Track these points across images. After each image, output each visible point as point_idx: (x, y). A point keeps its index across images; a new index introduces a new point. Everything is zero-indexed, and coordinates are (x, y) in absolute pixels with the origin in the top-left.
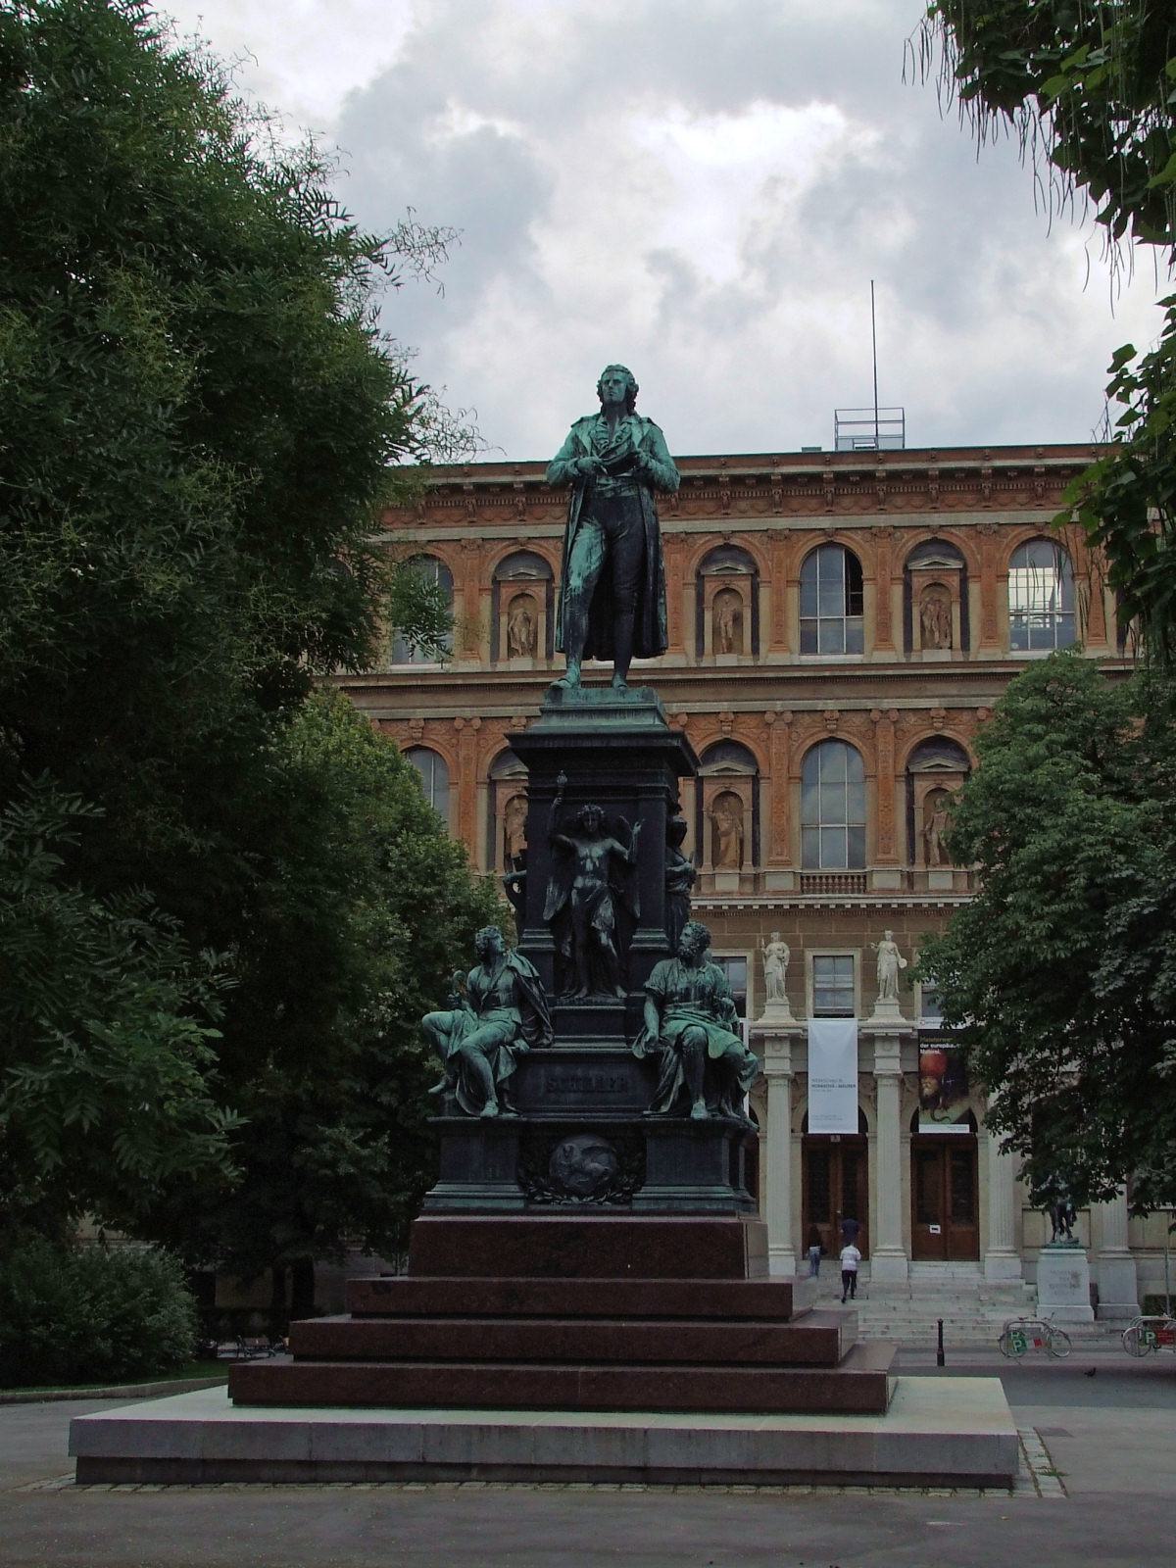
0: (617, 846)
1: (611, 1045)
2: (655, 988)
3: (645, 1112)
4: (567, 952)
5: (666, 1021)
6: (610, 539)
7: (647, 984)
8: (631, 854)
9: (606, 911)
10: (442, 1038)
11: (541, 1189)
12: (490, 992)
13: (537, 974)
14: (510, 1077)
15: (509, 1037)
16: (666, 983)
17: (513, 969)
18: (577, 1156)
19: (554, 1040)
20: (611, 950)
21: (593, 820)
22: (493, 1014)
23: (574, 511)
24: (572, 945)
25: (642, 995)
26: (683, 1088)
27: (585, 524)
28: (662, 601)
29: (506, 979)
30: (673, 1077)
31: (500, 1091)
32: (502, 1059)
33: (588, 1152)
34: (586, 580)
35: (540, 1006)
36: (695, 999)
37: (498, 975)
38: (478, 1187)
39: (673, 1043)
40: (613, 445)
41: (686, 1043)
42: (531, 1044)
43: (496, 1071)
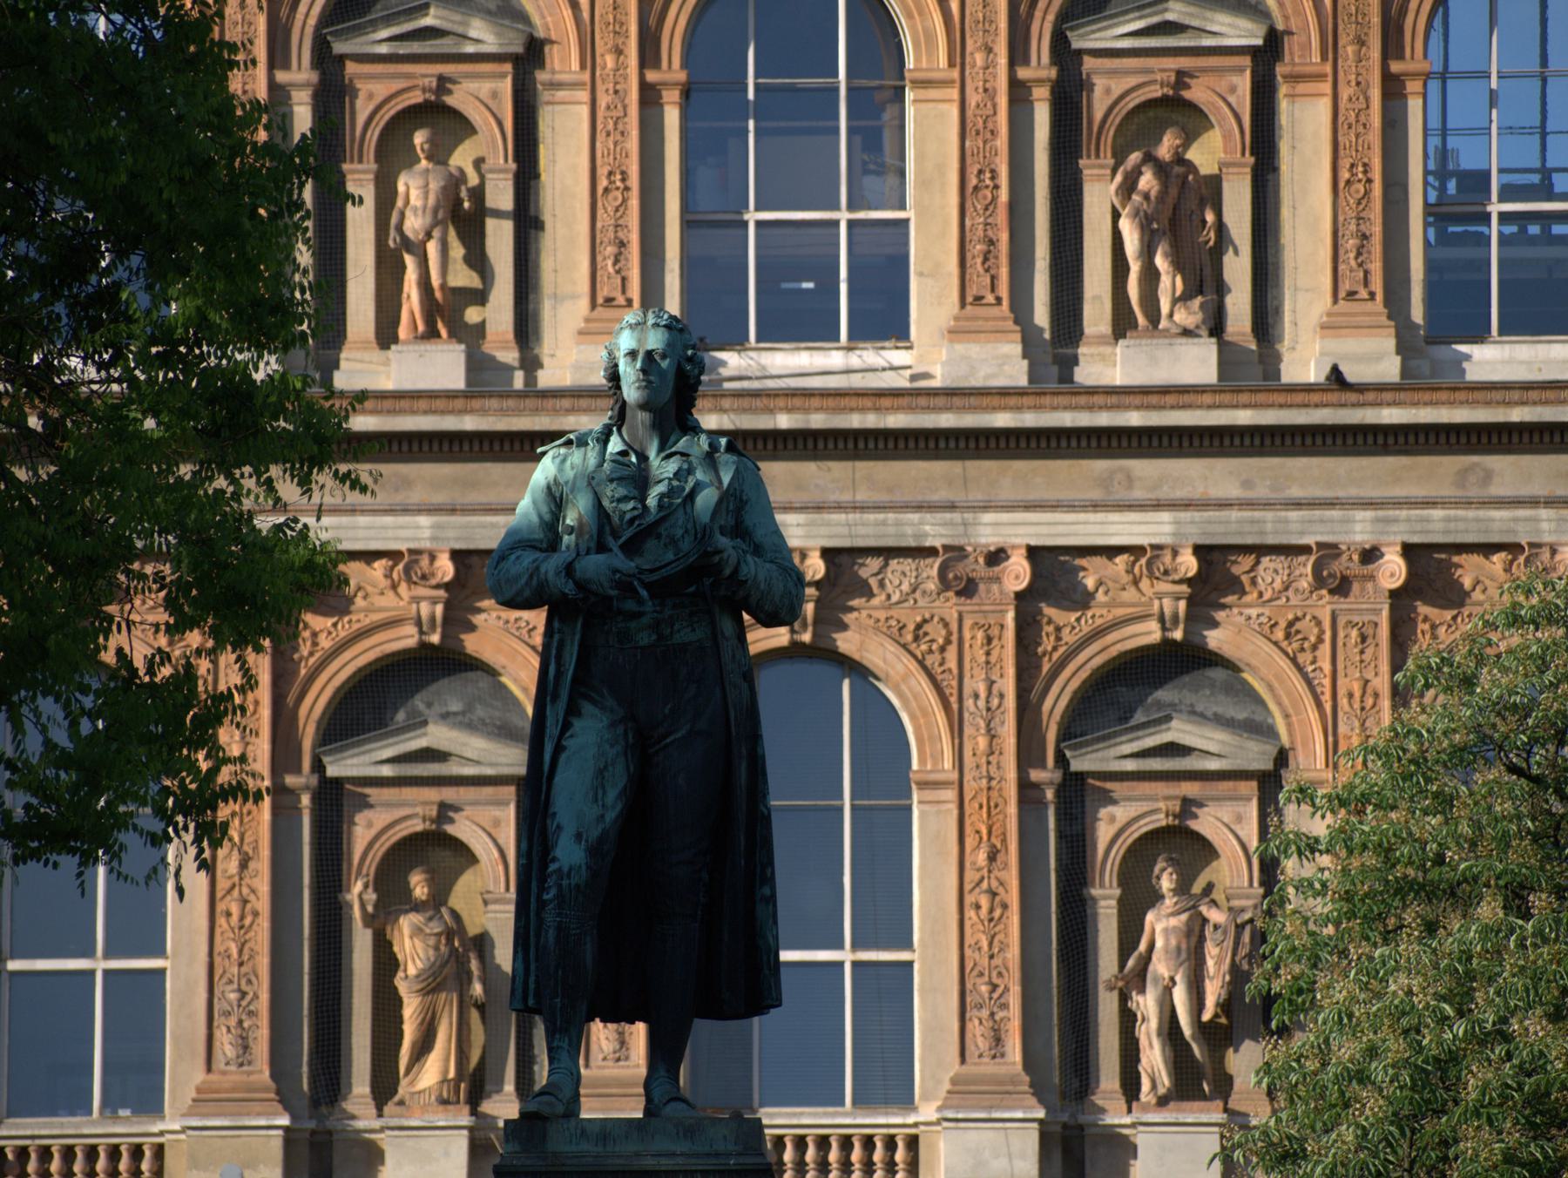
23: (559, 674)
27: (587, 708)
28: (767, 891)
34: (594, 851)
40: (650, 519)
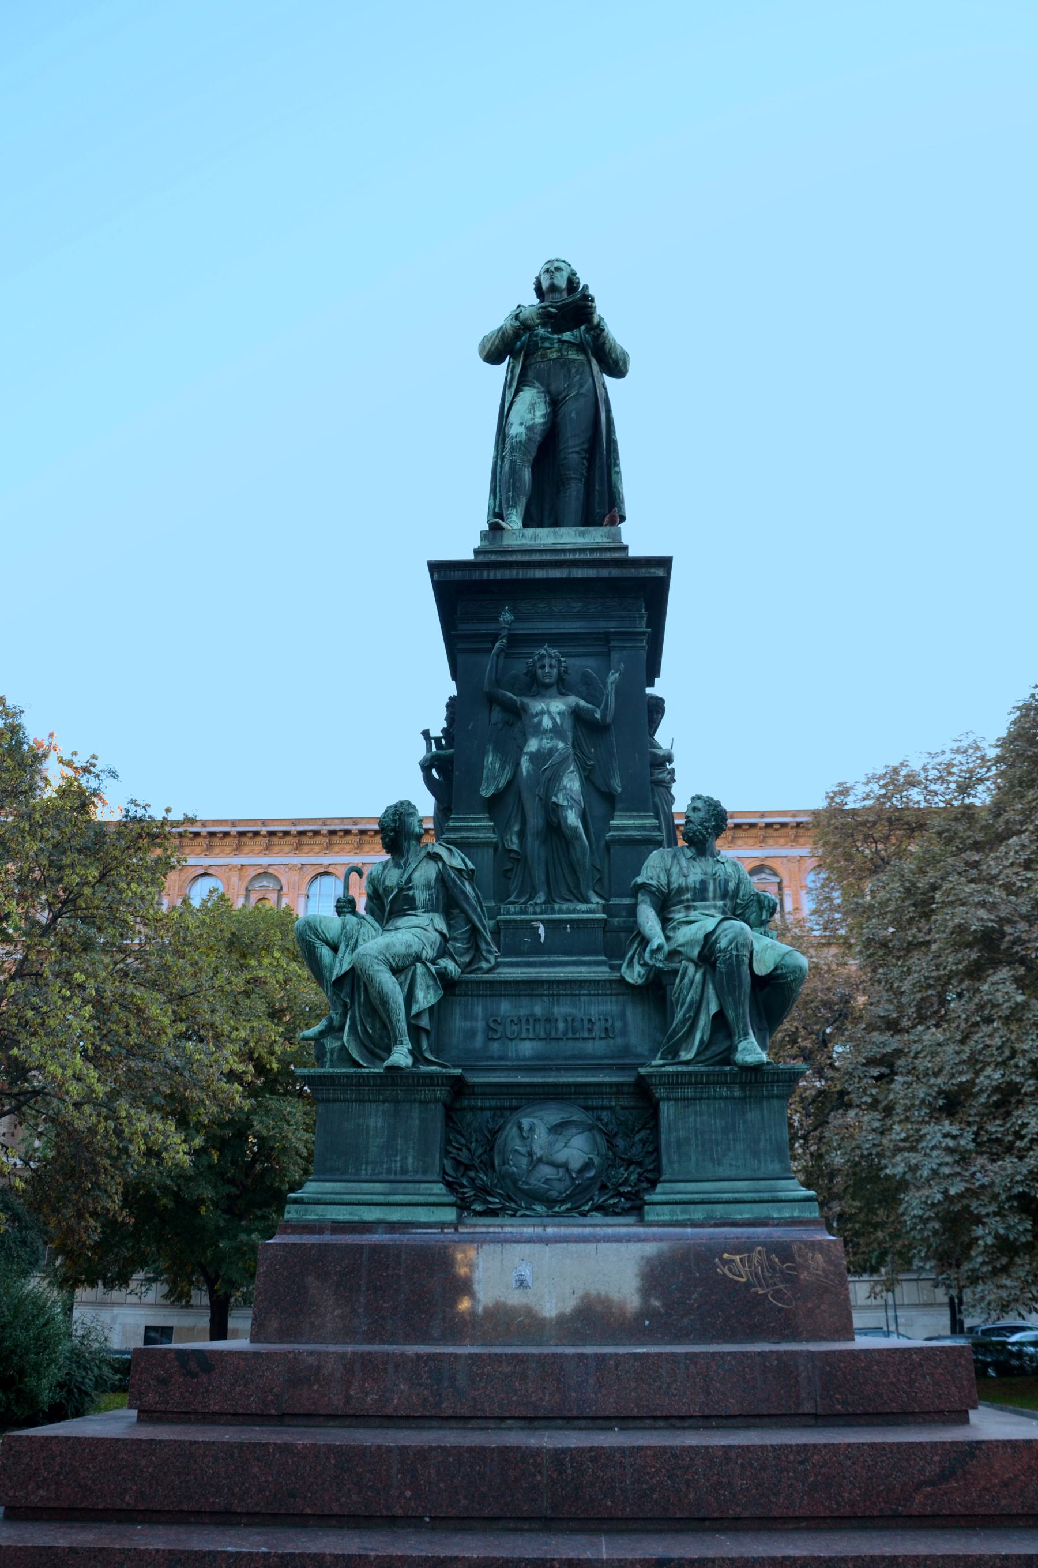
0: (582, 703)
1: (583, 969)
2: (654, 883)
3: (654, 1063)
4: (514, 844)
5: (674, 928)
6: (555, 403)
7: (639, 880)
8: (604, 714)
9: (572, 783)
10: (325, 952)
11: (485, 1191)
12: (401, 890)
13: (471, 866)
14: (431, 1008)
15: (429, 953)
16: (669, 876)
17: (435, 857)
18: (541, 1138)
19: (498, 965)
20: (580, 838)
21: (551, 666)
22: (402, 922)
24: (522, 834)
25: (627, 901)
26: (720, 1020)
28: (617, 469)
29: (425, 873)
30: (697, 1007)
31: (415, 1031)
32: (419, 980)
33: (557, 1129)
35: (475, 910)
36: (714, 899)
37: (413, 866)
38: (379, 1187)
39: (696, 952)
41: (723, 943)
42: (466, 968)
43: (410, 999)
